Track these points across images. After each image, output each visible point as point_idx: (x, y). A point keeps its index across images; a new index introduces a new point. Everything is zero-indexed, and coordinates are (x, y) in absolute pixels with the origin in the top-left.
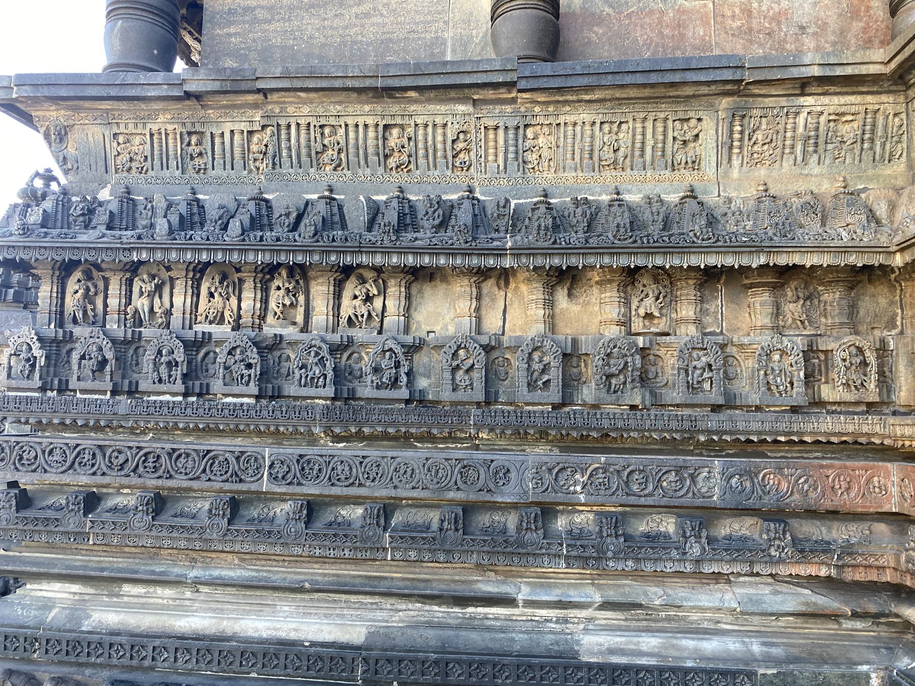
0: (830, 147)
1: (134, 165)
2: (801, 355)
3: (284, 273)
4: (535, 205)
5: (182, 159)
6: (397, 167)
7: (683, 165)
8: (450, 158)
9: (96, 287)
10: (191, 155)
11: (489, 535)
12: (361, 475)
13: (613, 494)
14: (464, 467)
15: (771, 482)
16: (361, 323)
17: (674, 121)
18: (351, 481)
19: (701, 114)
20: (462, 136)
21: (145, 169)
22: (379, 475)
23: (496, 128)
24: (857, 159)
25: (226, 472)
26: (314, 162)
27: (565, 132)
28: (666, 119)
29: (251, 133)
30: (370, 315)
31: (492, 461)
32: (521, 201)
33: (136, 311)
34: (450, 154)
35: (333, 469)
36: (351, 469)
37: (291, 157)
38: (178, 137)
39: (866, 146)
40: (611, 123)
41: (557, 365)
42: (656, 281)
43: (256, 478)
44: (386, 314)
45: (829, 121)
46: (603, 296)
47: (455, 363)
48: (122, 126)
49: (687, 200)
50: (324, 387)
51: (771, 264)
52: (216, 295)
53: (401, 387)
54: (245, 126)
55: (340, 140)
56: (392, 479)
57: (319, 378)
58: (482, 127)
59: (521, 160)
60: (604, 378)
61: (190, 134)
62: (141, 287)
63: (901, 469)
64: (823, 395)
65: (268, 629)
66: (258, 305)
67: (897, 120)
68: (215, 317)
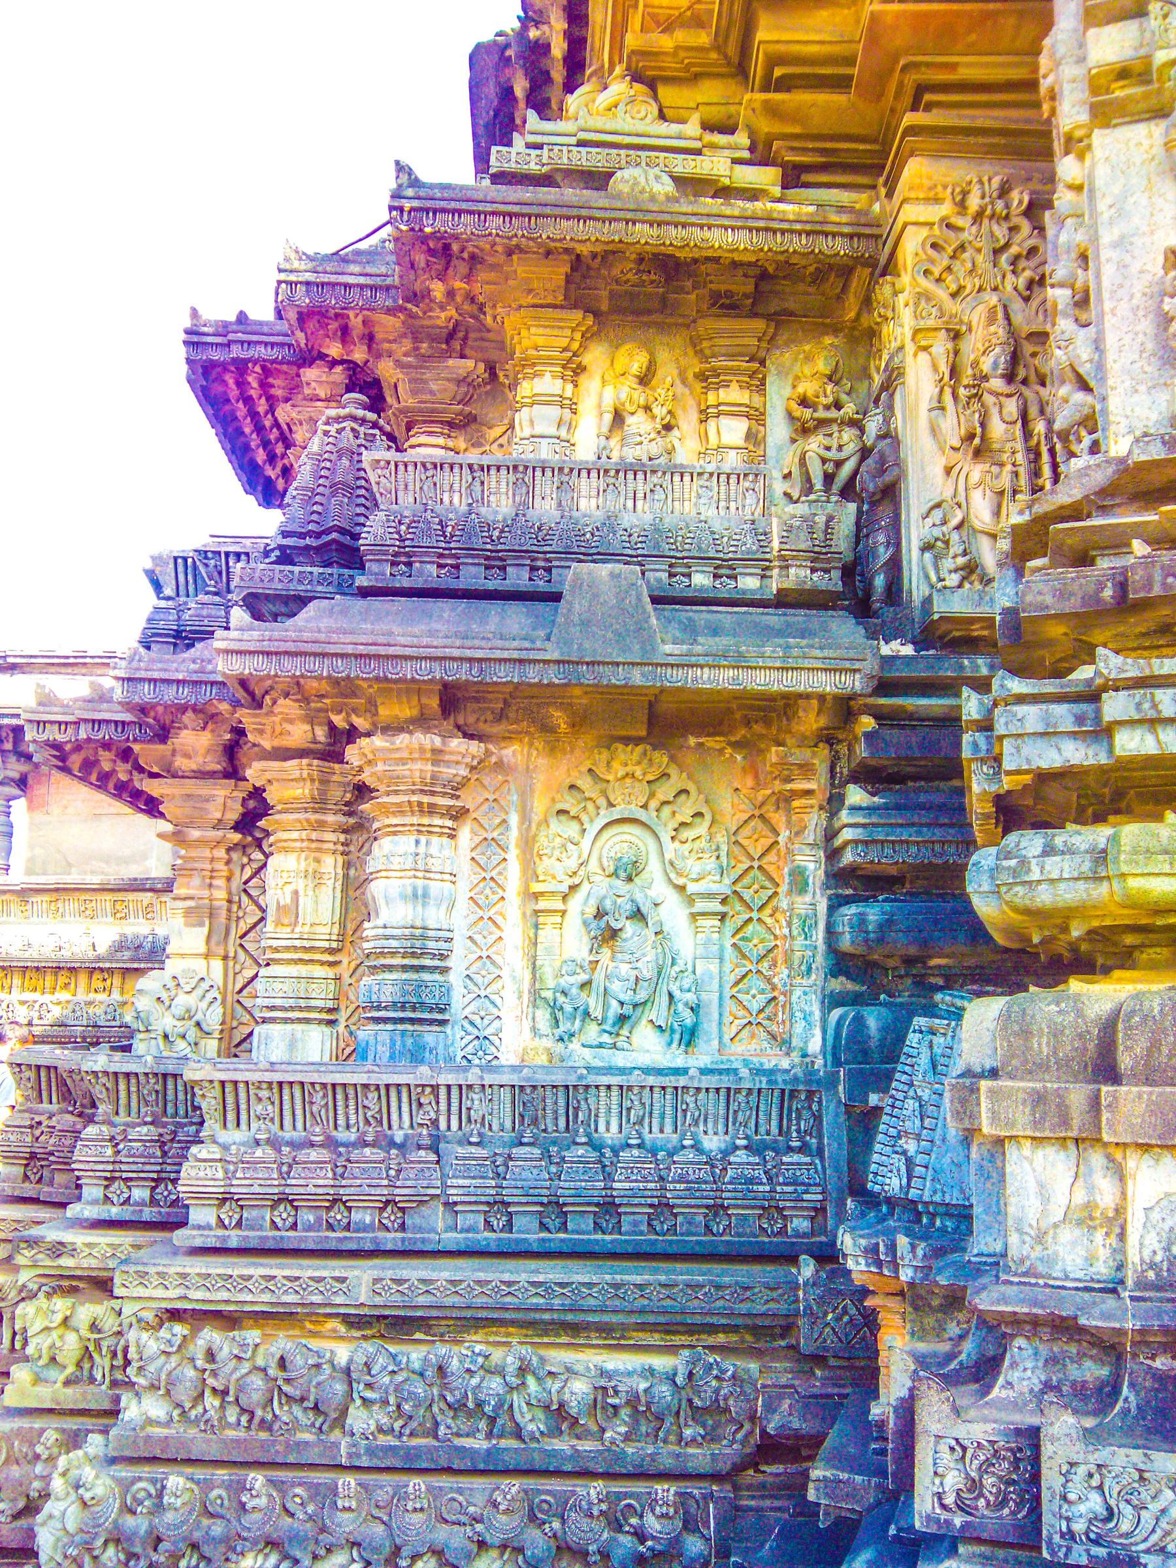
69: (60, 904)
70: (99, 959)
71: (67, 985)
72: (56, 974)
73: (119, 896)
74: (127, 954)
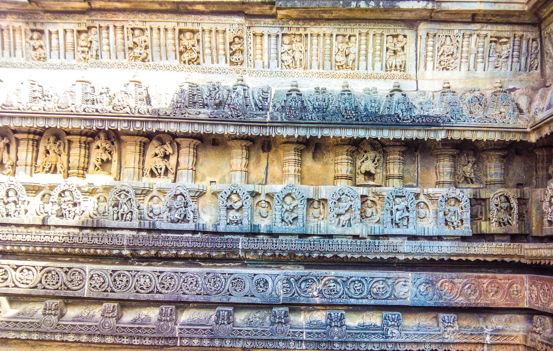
0: (492, 59)
2: (468, 201)
3: (102, 136)
4: (289, 91)
5: (26, 49)
6: (189, 61)
7: (393, 68)
8: (228, 56)
10: (34, 47)
12: (158, 285)
13: (340, 297)
14: (235, 279)
15: (447, 287)
16: (160, 174)
17: (387, 36)
18: (150, 290)
19: (407, 32)
20: (237, 40)
22: (172, 285)
23: (262, 35)
24: (510, 68)
25: (57, 283)
26: (127, 55)
27: (311, 40)
28: (382, 34)
29: (79, 32)
31: (255, 275)
32: (280, 89)
34: (228, 52)
36: (151, 280)
37: (109, 51)
38: (23, 32)
39: (515, 60)
40: (344, 36)
41: (303, 206)
42: (374, 148)
44: (179, 168)
45: (491, 42)
46: (336, 158)
47: (229, 204)
49: (395, 92)
50: (131, 221)
51: (449, 139)
52: (51, 152)
53: (188, 221)
54: (76, 28)
55: (146, 39)
56: (181, 288)
57: (127, 214)
59: (280, 60)
60: (335, 216)
61: (33, 31)
63: (531, 279)
64: (483, 228)
66: (82, 160)
67: (534, 43)
68: (50, 168)
69: (93, 35)
71: (105, 164)
72: (88, 146)
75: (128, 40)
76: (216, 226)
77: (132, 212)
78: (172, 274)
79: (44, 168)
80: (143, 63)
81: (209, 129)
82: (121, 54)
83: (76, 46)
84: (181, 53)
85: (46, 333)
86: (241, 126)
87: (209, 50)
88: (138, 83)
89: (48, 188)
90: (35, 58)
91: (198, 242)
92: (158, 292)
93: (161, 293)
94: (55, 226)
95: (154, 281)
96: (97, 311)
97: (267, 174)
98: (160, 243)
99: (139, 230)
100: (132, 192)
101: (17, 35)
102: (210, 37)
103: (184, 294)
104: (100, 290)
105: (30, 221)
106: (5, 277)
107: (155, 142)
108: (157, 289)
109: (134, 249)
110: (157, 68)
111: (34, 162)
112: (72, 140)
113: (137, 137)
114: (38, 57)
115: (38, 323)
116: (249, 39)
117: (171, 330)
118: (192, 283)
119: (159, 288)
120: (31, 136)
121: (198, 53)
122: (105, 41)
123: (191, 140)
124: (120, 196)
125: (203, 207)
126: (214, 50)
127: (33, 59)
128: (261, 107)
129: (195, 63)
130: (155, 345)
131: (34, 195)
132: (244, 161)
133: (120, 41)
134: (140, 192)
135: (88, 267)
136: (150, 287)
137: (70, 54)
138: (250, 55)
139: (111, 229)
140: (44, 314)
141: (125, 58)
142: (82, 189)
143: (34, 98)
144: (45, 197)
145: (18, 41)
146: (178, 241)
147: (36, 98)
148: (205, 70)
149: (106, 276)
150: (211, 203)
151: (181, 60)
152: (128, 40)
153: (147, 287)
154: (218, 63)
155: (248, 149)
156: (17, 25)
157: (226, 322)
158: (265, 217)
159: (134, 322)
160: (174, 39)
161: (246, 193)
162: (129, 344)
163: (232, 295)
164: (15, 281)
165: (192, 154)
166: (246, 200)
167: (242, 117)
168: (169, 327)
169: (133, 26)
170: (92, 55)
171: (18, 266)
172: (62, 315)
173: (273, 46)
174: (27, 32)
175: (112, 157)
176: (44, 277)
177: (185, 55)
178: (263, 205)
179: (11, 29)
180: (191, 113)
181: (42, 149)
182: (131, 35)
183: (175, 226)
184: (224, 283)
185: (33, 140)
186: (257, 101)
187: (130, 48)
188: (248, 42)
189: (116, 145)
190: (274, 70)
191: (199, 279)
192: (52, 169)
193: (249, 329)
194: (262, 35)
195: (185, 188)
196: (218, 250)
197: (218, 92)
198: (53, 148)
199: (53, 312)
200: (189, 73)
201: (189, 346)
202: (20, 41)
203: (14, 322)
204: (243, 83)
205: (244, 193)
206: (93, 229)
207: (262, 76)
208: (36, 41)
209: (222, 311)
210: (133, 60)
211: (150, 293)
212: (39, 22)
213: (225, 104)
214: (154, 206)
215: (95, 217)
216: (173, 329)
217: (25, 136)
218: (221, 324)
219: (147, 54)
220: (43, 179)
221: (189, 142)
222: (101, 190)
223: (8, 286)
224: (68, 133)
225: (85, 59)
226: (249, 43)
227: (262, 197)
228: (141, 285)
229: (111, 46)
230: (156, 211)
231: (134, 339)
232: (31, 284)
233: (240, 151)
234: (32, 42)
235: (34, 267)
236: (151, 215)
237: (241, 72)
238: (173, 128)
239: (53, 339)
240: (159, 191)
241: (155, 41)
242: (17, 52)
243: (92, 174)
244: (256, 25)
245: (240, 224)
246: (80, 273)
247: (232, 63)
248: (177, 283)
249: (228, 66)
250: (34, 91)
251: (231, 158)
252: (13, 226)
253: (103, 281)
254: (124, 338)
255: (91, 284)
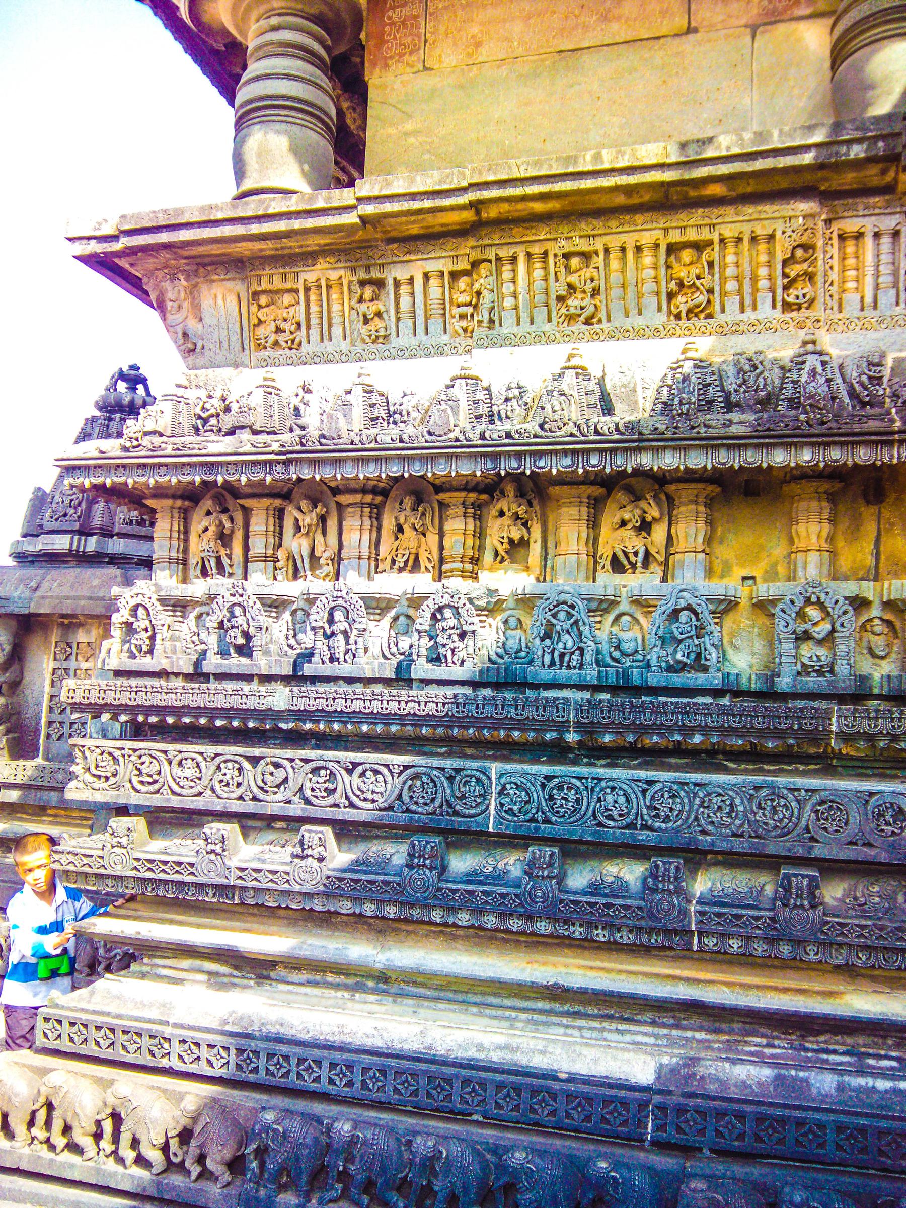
1: (281, 338)
3: (510, 489)
5: (351, 322)
6: (689, 311)
8: (779, 291)
9: (232, 520)
10: (365, 316)
11: (869, 917)
12: (645, 811)
14: (822, 803)
16: (634, 566)
20: (799, 253)
21: (297, 341)
23: (859, 236)
25: (433, 800)
26: (554, 314)
29: (455, 276)
30: (647, 554)
31: (871, 794)
33: (291, 557)
34: (780, 282)
35: (599, 800)
36: (627, 800)
37: (516, 308)
38: (345, 289)
43: (478, 810)
47: (801, 628)
48: (265, 280)
50: (581, 668)
52: (406, 527)
54: (446, 266)
55: (595, 274)
56: (696, 819)
57: (573, 653)
58: (835, 236)
61: (363, 284)
62: (297, 520)
65: (499, 1048)
66: (470, 542)
69: (483, 280)
70: (635, 439)
71: (516, 548)
72: (478, 512)
73: (690, 226)
74: (741, 422)
75: (557, 280)
76: (772, 676)
77: (581, 650)
78: (675, 787)
79: (394, 562)
80: (587, 327)
81: (752, 458)
82: (541, 314)
83: (448, 306)
84: (671, 296)
85: (412, 906)
86: (828, 444)
87: (736, 283)
88: (582, 372)
89: (405, 603)
90: (368, 340)
91: (734, 716)
92: (646, 827)
93: (651, 829)
94: (422, 681)
95: (635, 800)
96: (512, 863)
97: (877, 557)
98: (647, 718)
99: (596, 688)
100: (581, 605)
101: (335, 296)
102: (736, 254)
103: (704, 832)
104: (522, 818)
105: (373, 670)
106: (331, 787)
107: (621, 496)
108: (642, 820)
109: (588, 729)
110: (618, 335)
111: (374, 551)
112: (446, 502)
113: (583, 487)
114: (373, 337)
115: (399, 885)
116: (829, 248)
117: (679, 911)
118: (720, 808)
119: (646, 817)
120: (368, 498)
121: (711, 291)
122: (508, 288)
123: (701, 485)
124: (554, 616)
125: (732, 635)
126: (747, 283)
127: (364, 341)
128: (867, 399)
129: (702, 316)
130: (642, 945)
131: (377, 617)
132: (826, 528)
133: (539, 285)
134: (594, 605)
135: (494, 768)
136: (628, 813)
137: (436, 324)
138: (831, 285)
139: (536, 686)
140: (410, 866)
141: (550, 321)
142: (476, 602)
143: (372, 420)
144: (399, 622)
145: (336, 307)
146: (687, 713)
147: (377, 418)
148: (726, 329)
149: (533, 789)
150: (753, 626)
151: (670, 312)
152: (557, 280)
153: (621, 815)
154: (755, 308)
155: (833, 499)
156: (334, 275)
157: (806, 903)
158: (882, 658)
159: (595, 889)
160: (655, 267)
161: (841, 601)
162: (586, 939)
163: (817, 841)
164: (350, 794)
165: (702, 518)
166: (843, 618)
167: (834, 425)
168: (674, 906)
169: (568, 247)
170: (480, 322)
171: (355, 765)
172: (444, 868)
173: (885, 258)
174: (353, 288)
175: (529, 532)
176: (406, 787)
177: (680, 299)
178: (877, 629)
179: (323, 284)
180: (713, 423)
181: (388, 523)
182: (562, 269)
183: (677, 679)
184: (796, 811)
185: (370, 505)
186: (856, 386)
187: (560, 299)
188: (827, 255)
189: (537, 508)
190: (888, 313)
191: (738, 801)
192: (410, 563)
193: (863, 922)
194: (859, 236)
195: (697, 594)
196: (778, 734)
197: (761, 373)
198: (413, 520)
199: (428, 862)
200: (690, 339)
201: (718, 952)
202: (340, 308)
203: (352, 880)
204: (818, 349)
205: (837, 602)
206: (497, 686)
207: (858, 328)
208: (370, 304)
209: (796, 875)
210: (565, 324)
211: (627, 827)
212: (375, 265)
213: (778, 400)
214: (622, 635)
215: (500, 661)
216: (684, 912)
217: (358, 498)
218: (795, 906)
219: (596, 306)
220: (393, 584)
221: (695, 492)
222: (511, 603)
223: (336, 805)
224: (438, 489)
225: (465, 330)
226: (828, 256)
227: (875, 611)
228: (607, 810)
229: (520, 297)
230: (628, 647)
231: (597, 928)
232: (381, 802)
233: (814, 504)
234: (363, 308)
235: (387, 766)
236: (617, 654)
237: (809, 323)
238: (670, 461)
239: (427, 919)
240: (633, 602)
241: (615, 278)
242: (333, 329)
243: (491, 569)
244: (845, 214)
245: (827, 675)
246: (478, 780)
247: (787, 307)
248: (687, 808)
249: (778, 313)
250: (372, 406)
251: (792, 521)
252: (341, 682)
253: (527, 799)
254: (574, 925)
255: (502, 805)
